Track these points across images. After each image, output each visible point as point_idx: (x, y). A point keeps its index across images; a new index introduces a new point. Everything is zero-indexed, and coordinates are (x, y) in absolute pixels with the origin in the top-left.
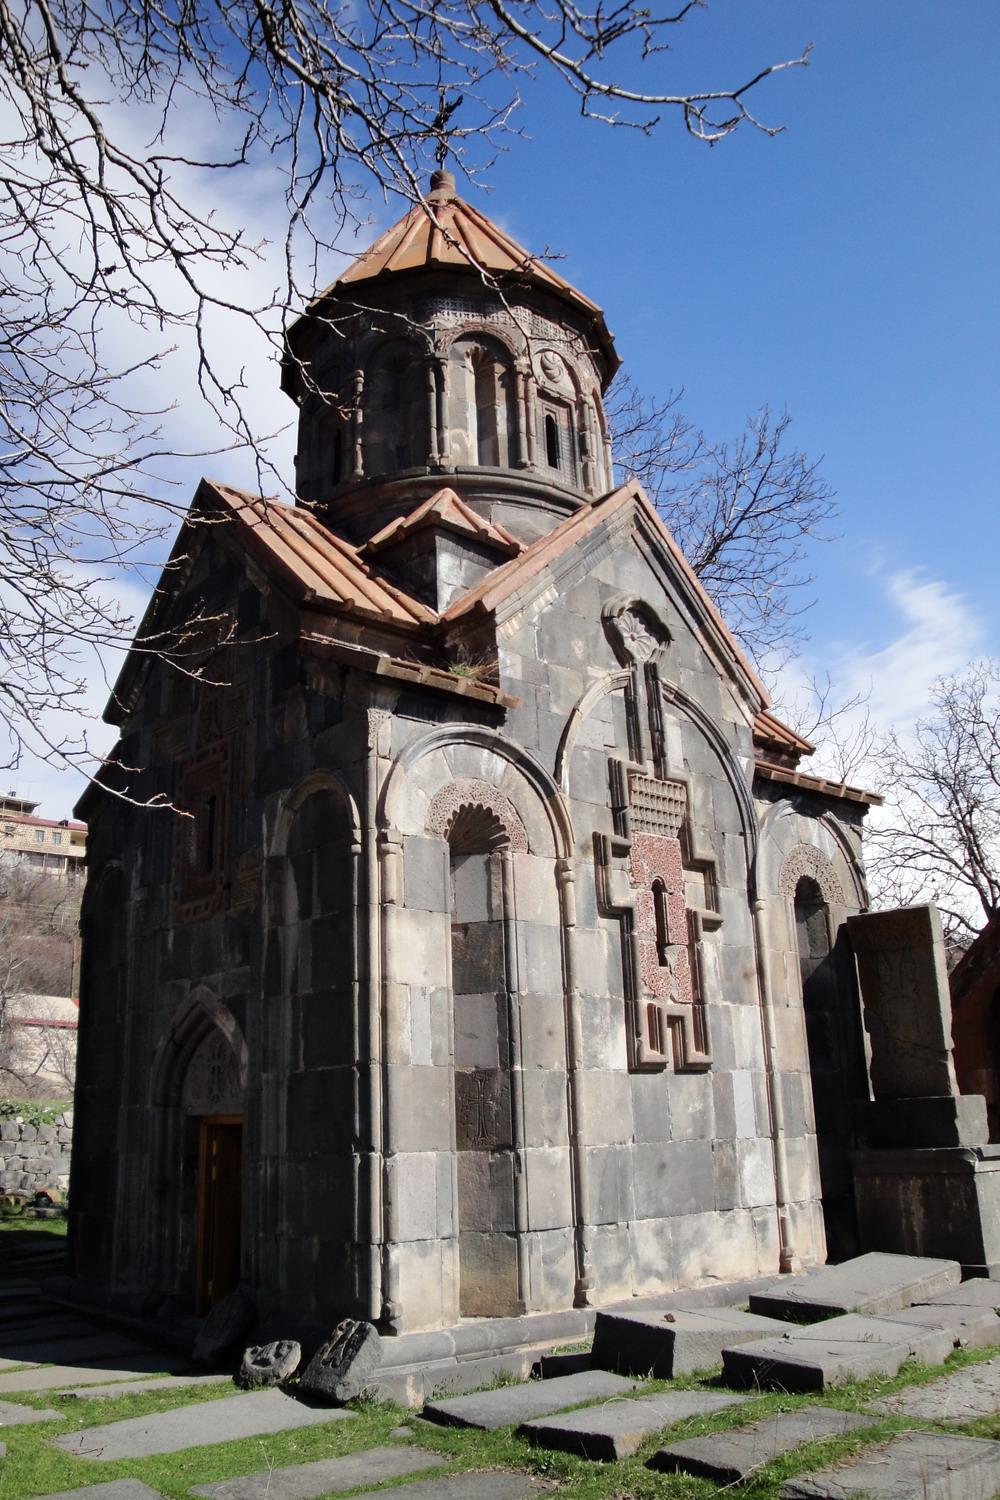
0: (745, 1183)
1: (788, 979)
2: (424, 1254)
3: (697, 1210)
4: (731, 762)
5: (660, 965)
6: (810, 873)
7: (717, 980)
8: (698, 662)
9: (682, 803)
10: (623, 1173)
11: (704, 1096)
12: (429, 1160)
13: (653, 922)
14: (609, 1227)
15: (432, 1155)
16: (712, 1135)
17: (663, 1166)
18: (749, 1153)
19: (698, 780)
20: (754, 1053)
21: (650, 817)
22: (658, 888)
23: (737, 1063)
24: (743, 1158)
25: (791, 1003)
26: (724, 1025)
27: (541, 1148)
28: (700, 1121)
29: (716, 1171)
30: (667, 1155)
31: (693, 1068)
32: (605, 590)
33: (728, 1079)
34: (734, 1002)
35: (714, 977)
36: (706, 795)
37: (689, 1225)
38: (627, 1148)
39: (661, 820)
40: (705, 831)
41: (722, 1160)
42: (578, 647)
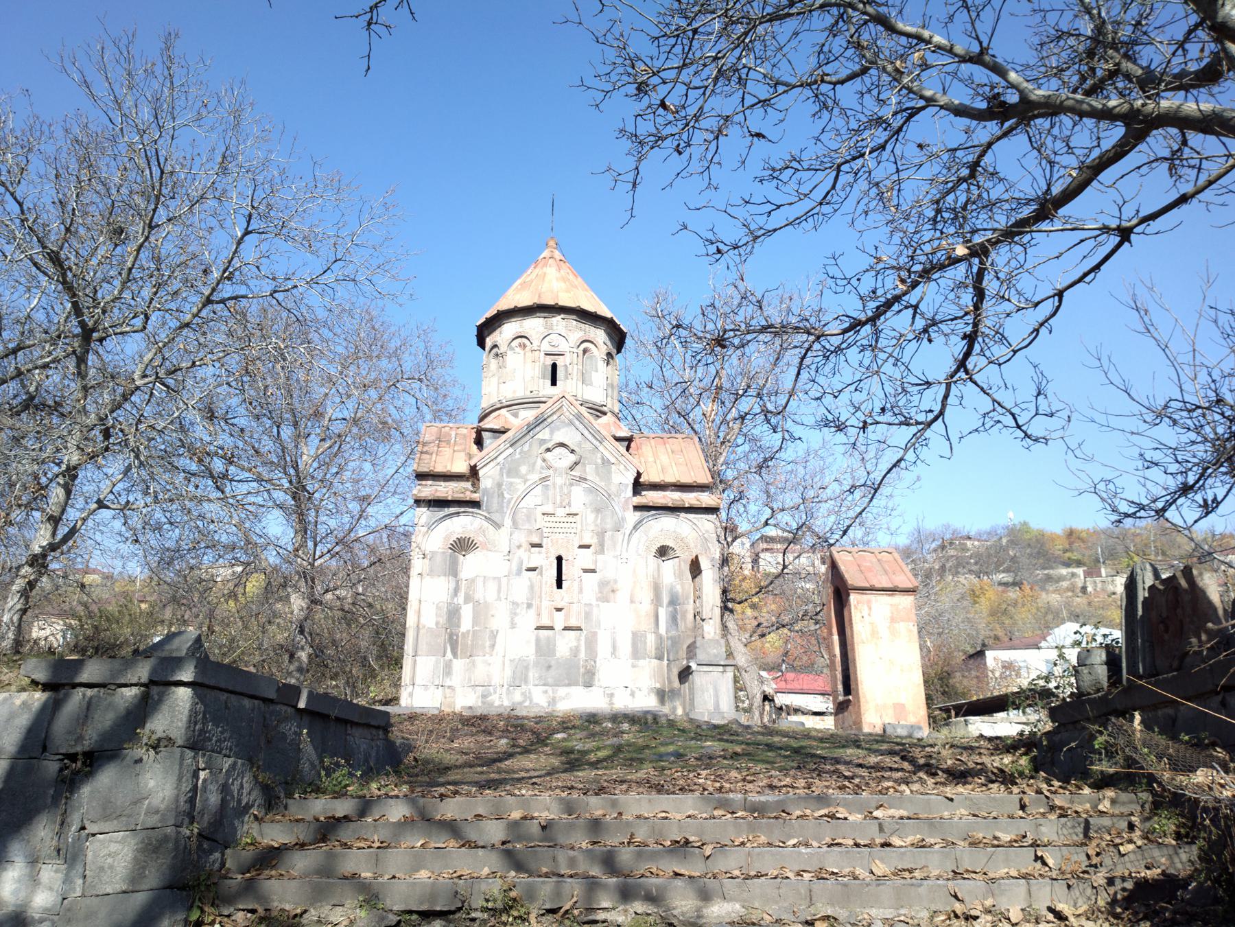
3: (569, 685)
6: (671, 544)
8: (599, 461)
10: (527, 668)
11: (579, 640)
16: (582, 655)
17: (549, 667)
22: (559, 559)
26: (595, 611)
28: (575, 652)
29: (582, 670)
30: (553, 663)
32: (543, 442)
33: (595, 634)
36: (597, 517)
37: (562, 691)
42: (523, 469)
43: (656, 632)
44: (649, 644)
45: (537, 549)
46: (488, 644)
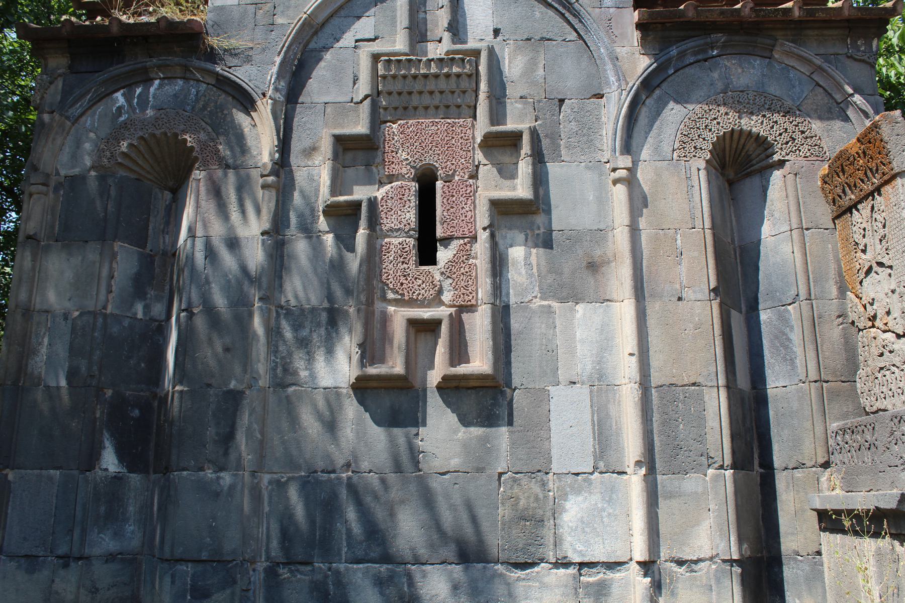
0: (564, 531)
1: (685, 263)
2: (31, 570)
4: (577, 15)
5: (422, 263)
7: (531, 275)
9: (470, 76)
12: (50, 478)
13: (410, 216)
14: (302, 568)
15: (56, 473)
18: (578, 492)
19: (518, 49)
20: (600, 361)
21: (415, 100)
23: (562, 375)
24: (564, 497)
25: (687, 294)
26: (539, 327)
27: (202, 473)
31: (463, 384)
34: (562, 300)
35: (523, 271)
38: (339, 479)
39: (437, 99)
40: (525, 104)
41: (518, 499)
43: (730, 386)
44: (712, 422)
45: (360, 155)
46: (211, 432)
